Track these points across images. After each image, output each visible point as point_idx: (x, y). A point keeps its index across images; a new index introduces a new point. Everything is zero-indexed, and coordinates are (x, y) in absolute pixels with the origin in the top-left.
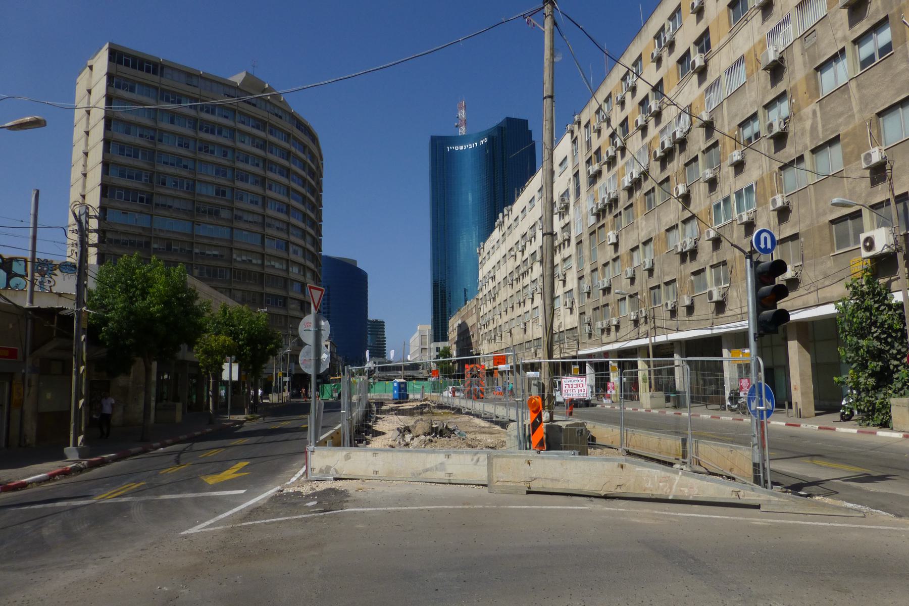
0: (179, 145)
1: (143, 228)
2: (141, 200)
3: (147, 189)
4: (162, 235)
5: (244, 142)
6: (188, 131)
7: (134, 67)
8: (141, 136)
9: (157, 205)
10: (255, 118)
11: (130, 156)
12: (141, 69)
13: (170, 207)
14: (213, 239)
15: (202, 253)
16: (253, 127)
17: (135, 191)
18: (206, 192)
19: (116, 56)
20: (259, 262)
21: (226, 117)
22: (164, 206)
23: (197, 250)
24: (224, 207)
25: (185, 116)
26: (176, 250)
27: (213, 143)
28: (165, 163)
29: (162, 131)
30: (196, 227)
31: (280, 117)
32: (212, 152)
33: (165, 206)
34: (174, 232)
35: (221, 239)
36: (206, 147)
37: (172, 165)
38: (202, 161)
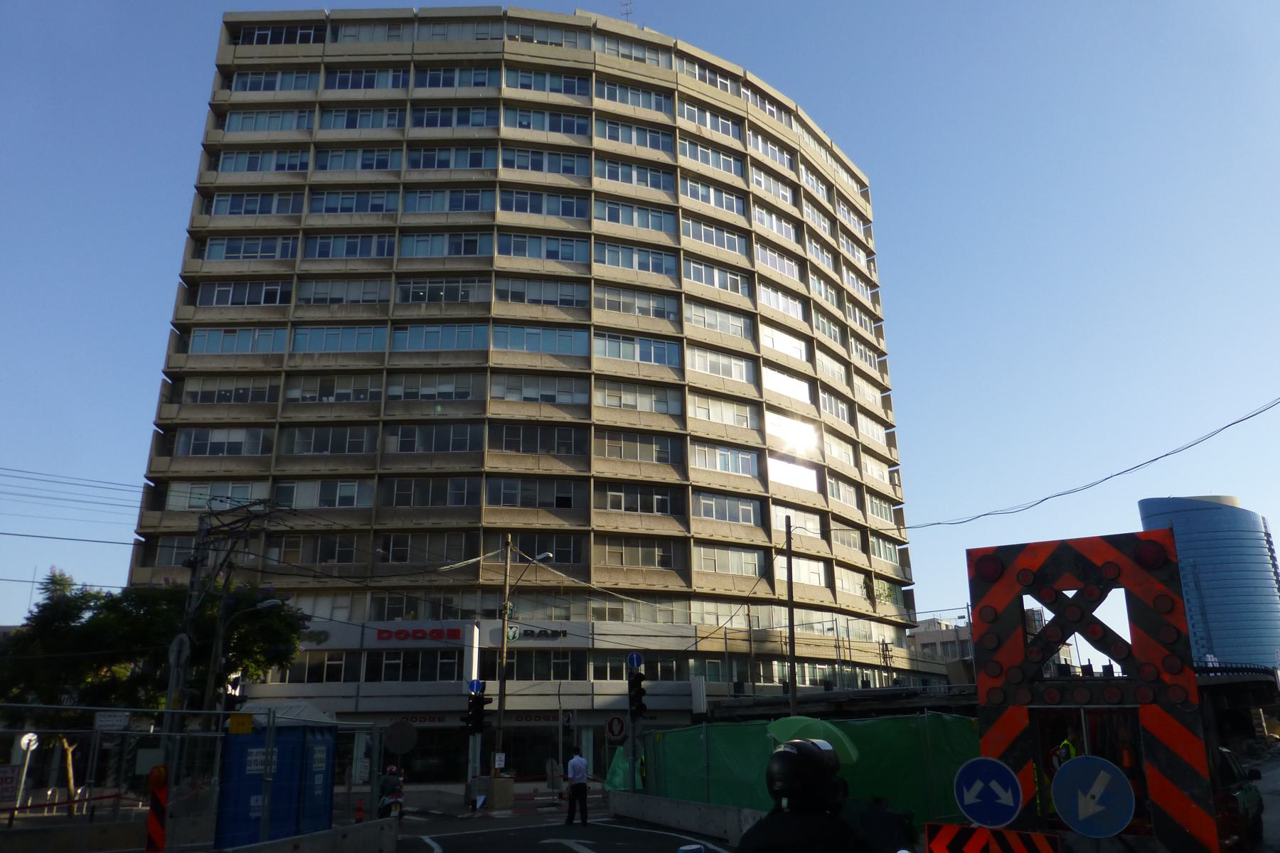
0: (365, 166)
1: (266, 358)
2: (270, 297)
3: (281, 270)
4: (307, 365)
5: (528, 127)
6: (383, 132)
7: (276, 40)
8: (280, 167)
9: (308, 301)
10: (556, 71)
11: (253, 212)
12: (290, 40)
13: (339, 301)
14: (436, 355)
15: (407, 395)
16: (552, 90)
17: (256, 279)
18: (432, 255)
19: (238, 31)
20: (580, 399)
21: (483, 84)
22: (316, 300)
23: (397, 390)
24: (468, 276)
25: (377, 105)
26: (347, 396)
27: (445, 144)
28: (334, 210)
29: (323, 149)
30: (400, 334)
31: (643, 60)
32: (444, 164)
33: (323, 300)
34: (336, 355)
35: (457, 354)
36: (424, 152)
37: (349, 210)
38: (410, 188)
